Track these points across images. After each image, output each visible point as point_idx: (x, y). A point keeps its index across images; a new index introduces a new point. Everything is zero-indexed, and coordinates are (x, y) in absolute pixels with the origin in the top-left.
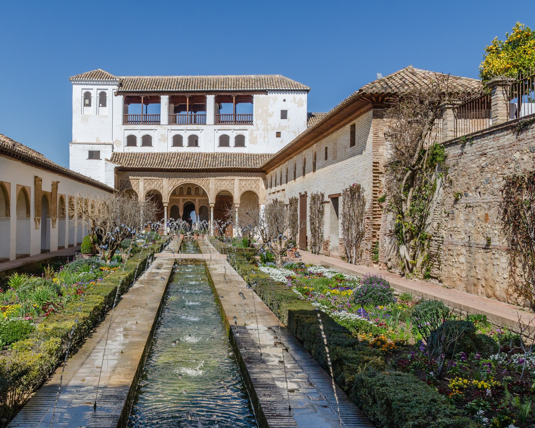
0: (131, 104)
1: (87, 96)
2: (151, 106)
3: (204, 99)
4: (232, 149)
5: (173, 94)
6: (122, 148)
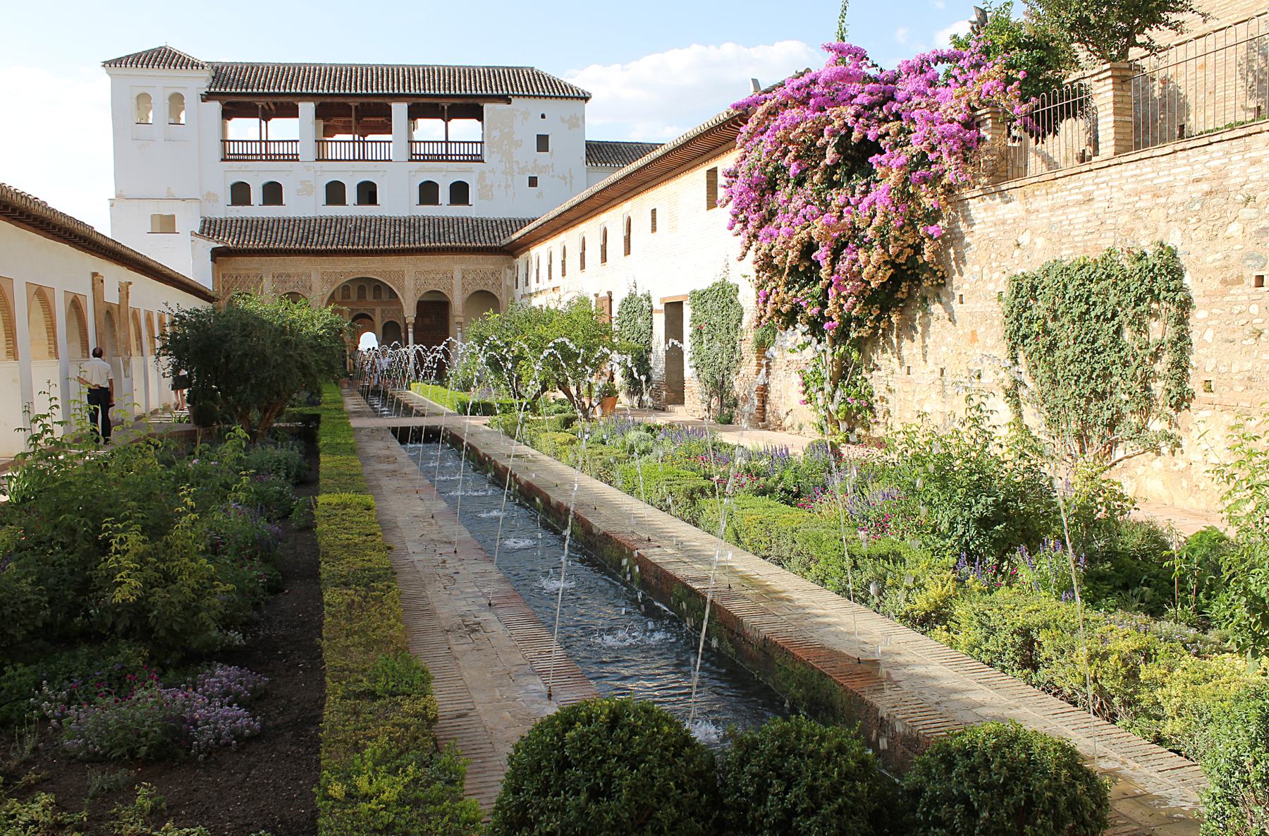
0: (234, 120)
1: (143, 99)
2: (274, 122)
3: (388, 113)
4: (444, 209)
5: (322, 100)
6: (224, 210)
